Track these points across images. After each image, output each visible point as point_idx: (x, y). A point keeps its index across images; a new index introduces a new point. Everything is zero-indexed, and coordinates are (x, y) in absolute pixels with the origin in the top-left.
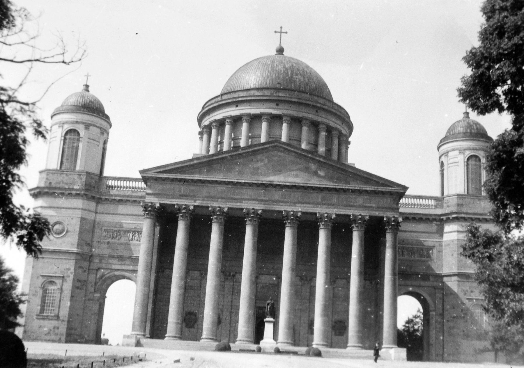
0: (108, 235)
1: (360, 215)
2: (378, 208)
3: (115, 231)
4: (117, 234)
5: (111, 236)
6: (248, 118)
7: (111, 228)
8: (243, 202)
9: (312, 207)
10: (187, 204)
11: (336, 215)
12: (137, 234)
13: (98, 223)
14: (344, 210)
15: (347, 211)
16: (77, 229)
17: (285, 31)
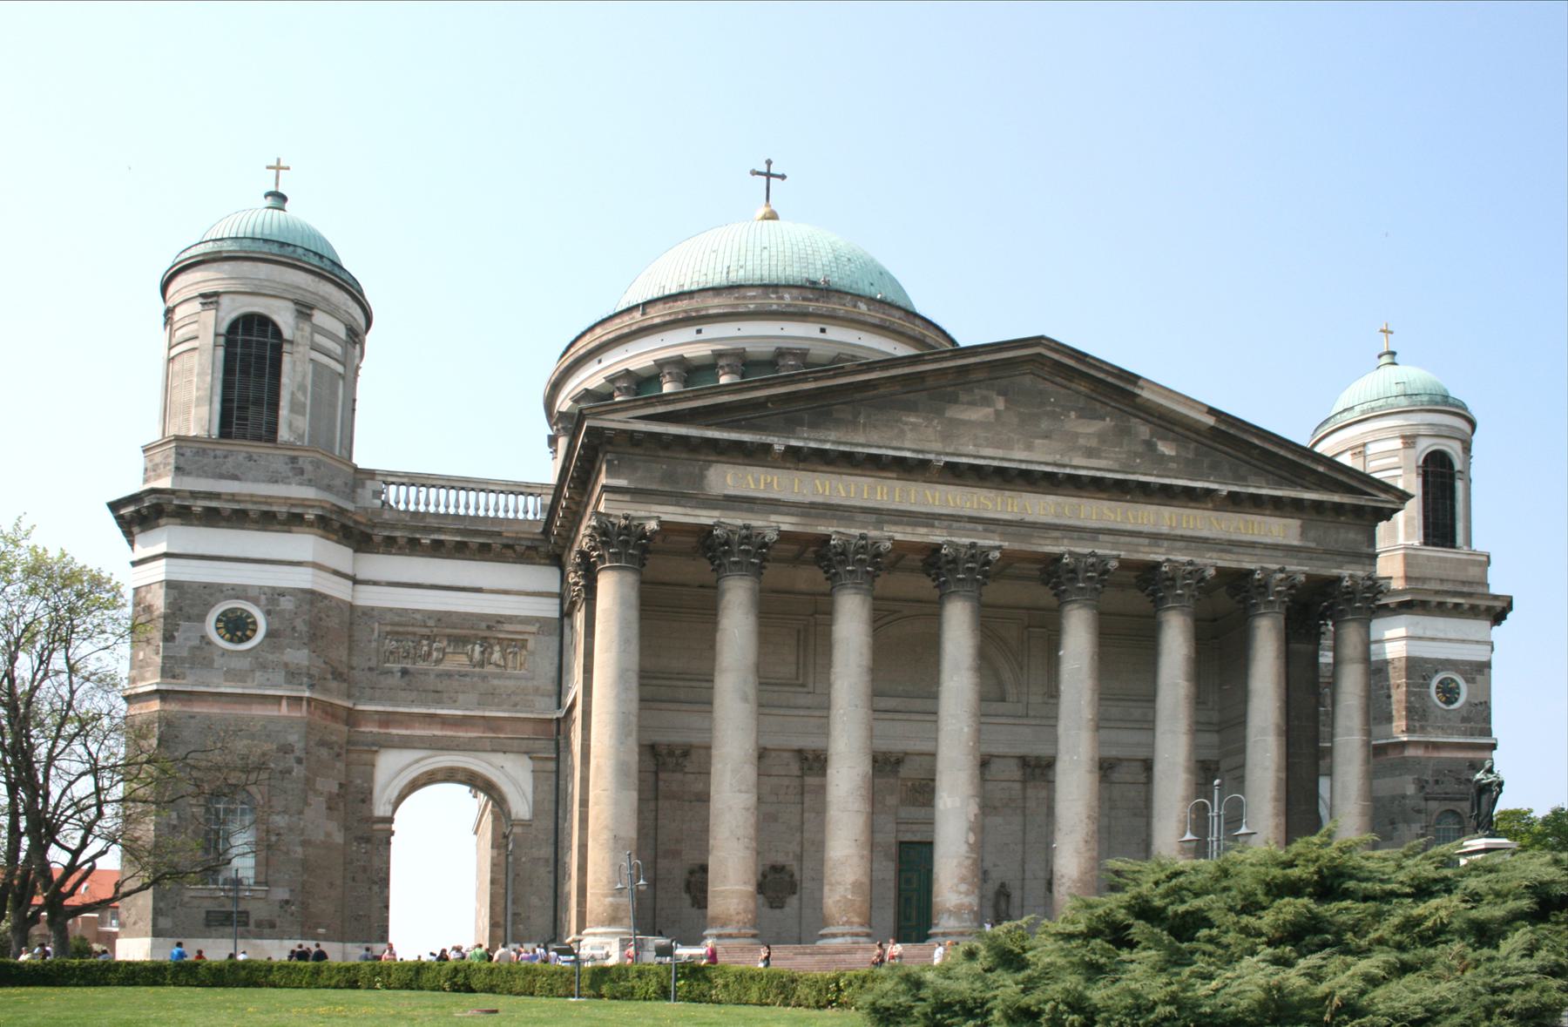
0: (401, 650)
1: (1282, 570)
2: (1326, 552)
3: (423, 637)
4: (430, 646)
5: (412, 651)
6: (677, 371)
7: (410, 629)
8: (936, 523)
9: (1145, 546)
10: (754, 523)
11: (1219, 570)
12: (497, 648)
13: (364, 613)
14: (1234, 557)
15: (1241, 557)
16: (301, 625)
17: (766, 166)
